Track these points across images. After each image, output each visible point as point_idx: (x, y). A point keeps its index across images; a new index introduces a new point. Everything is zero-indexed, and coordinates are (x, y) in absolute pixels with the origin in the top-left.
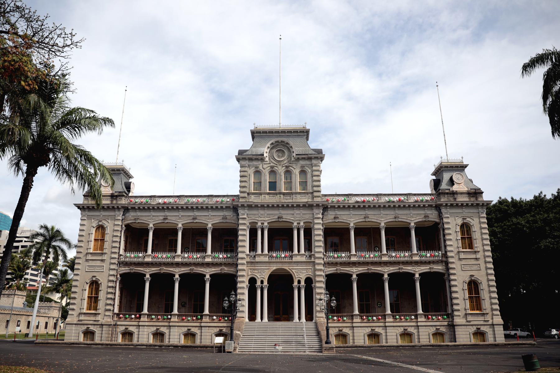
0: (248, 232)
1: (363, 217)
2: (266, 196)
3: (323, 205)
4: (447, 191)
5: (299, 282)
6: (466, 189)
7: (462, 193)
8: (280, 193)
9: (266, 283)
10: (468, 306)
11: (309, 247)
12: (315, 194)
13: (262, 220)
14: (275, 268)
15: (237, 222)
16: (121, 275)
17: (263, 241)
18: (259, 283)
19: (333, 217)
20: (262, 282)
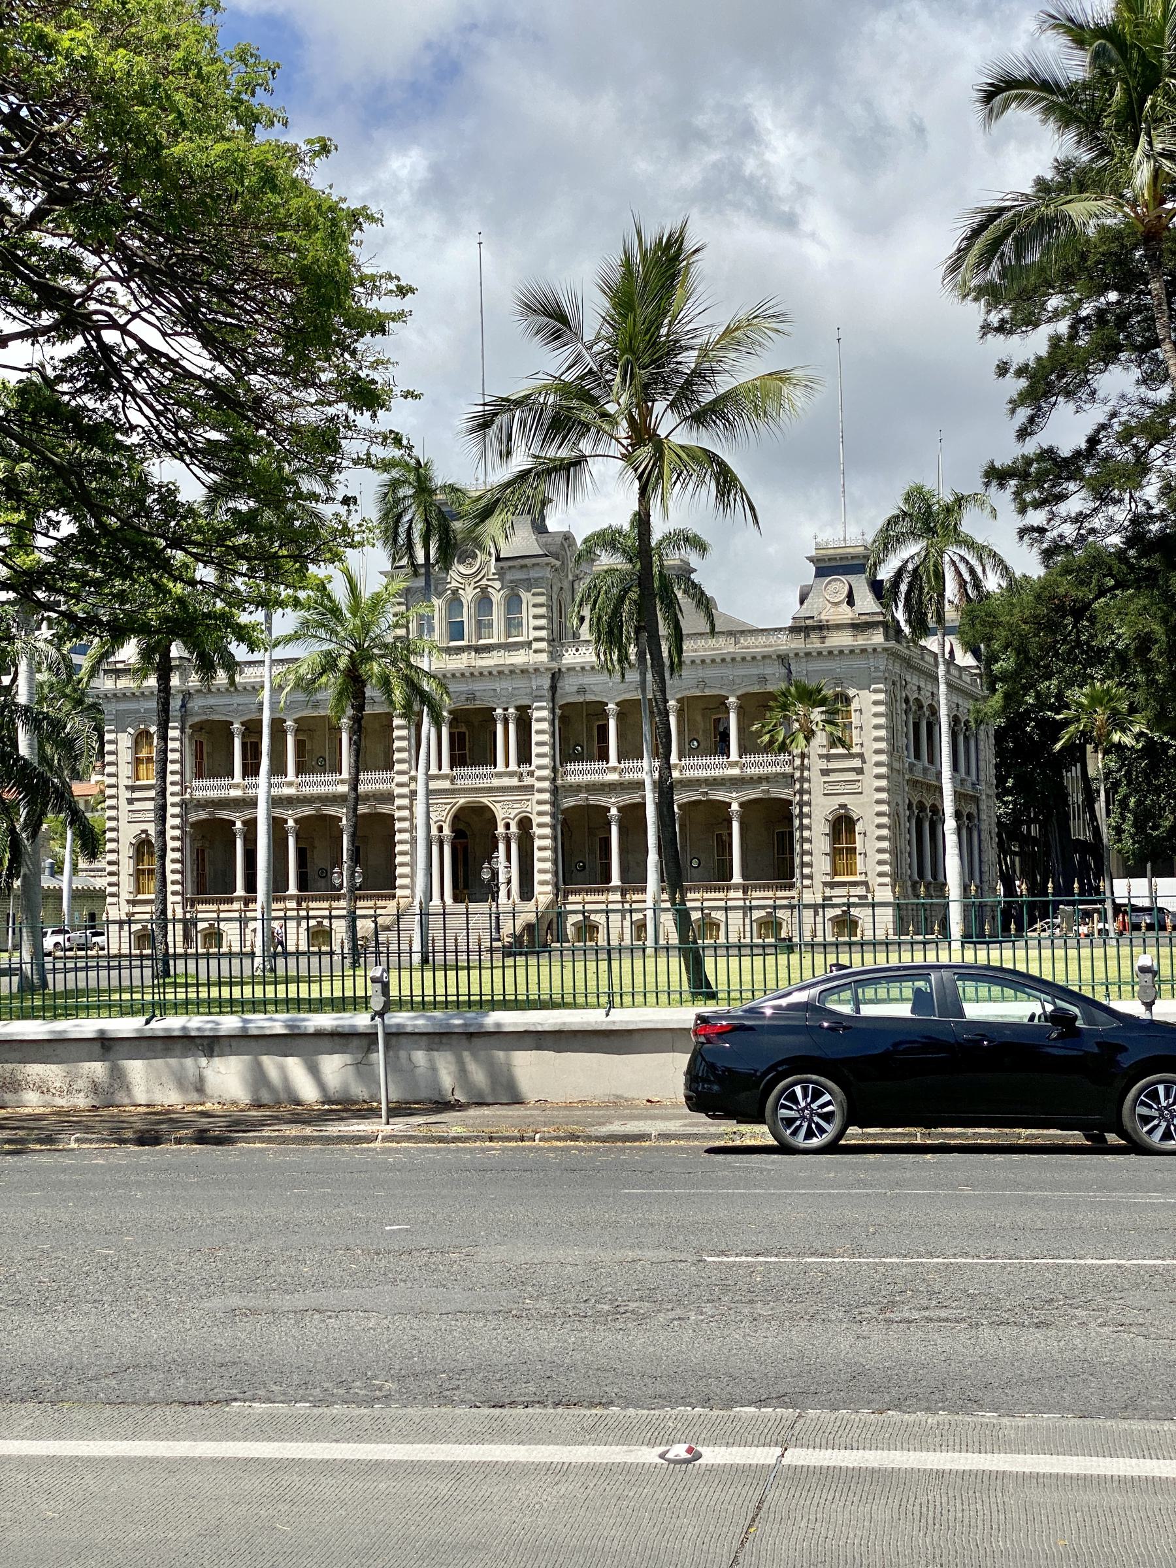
4: (809, 622)
5: (508, 826)
6: (851, 615)
7: (838, 627)
8: (469, 648)
9: (447, 831)
10: (828, 869)
11: (524, 757)
12: (535, 645)
14: (462, 801)
19: (575, 688)
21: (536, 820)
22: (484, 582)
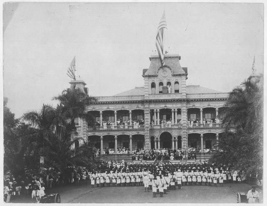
0: (150, 114)
1: (207, 105)
2: (158, 95)
3: (186, 100)
5: (175, 138)
9: (159, 139)
13: (156, 108)
14: (163, 132)
15: (143, 109)
16: (88, 137)
17: (157, 119)
18: (155, 139)
20: (157, 138)
21: (183, 136)
22: (169, 78)
